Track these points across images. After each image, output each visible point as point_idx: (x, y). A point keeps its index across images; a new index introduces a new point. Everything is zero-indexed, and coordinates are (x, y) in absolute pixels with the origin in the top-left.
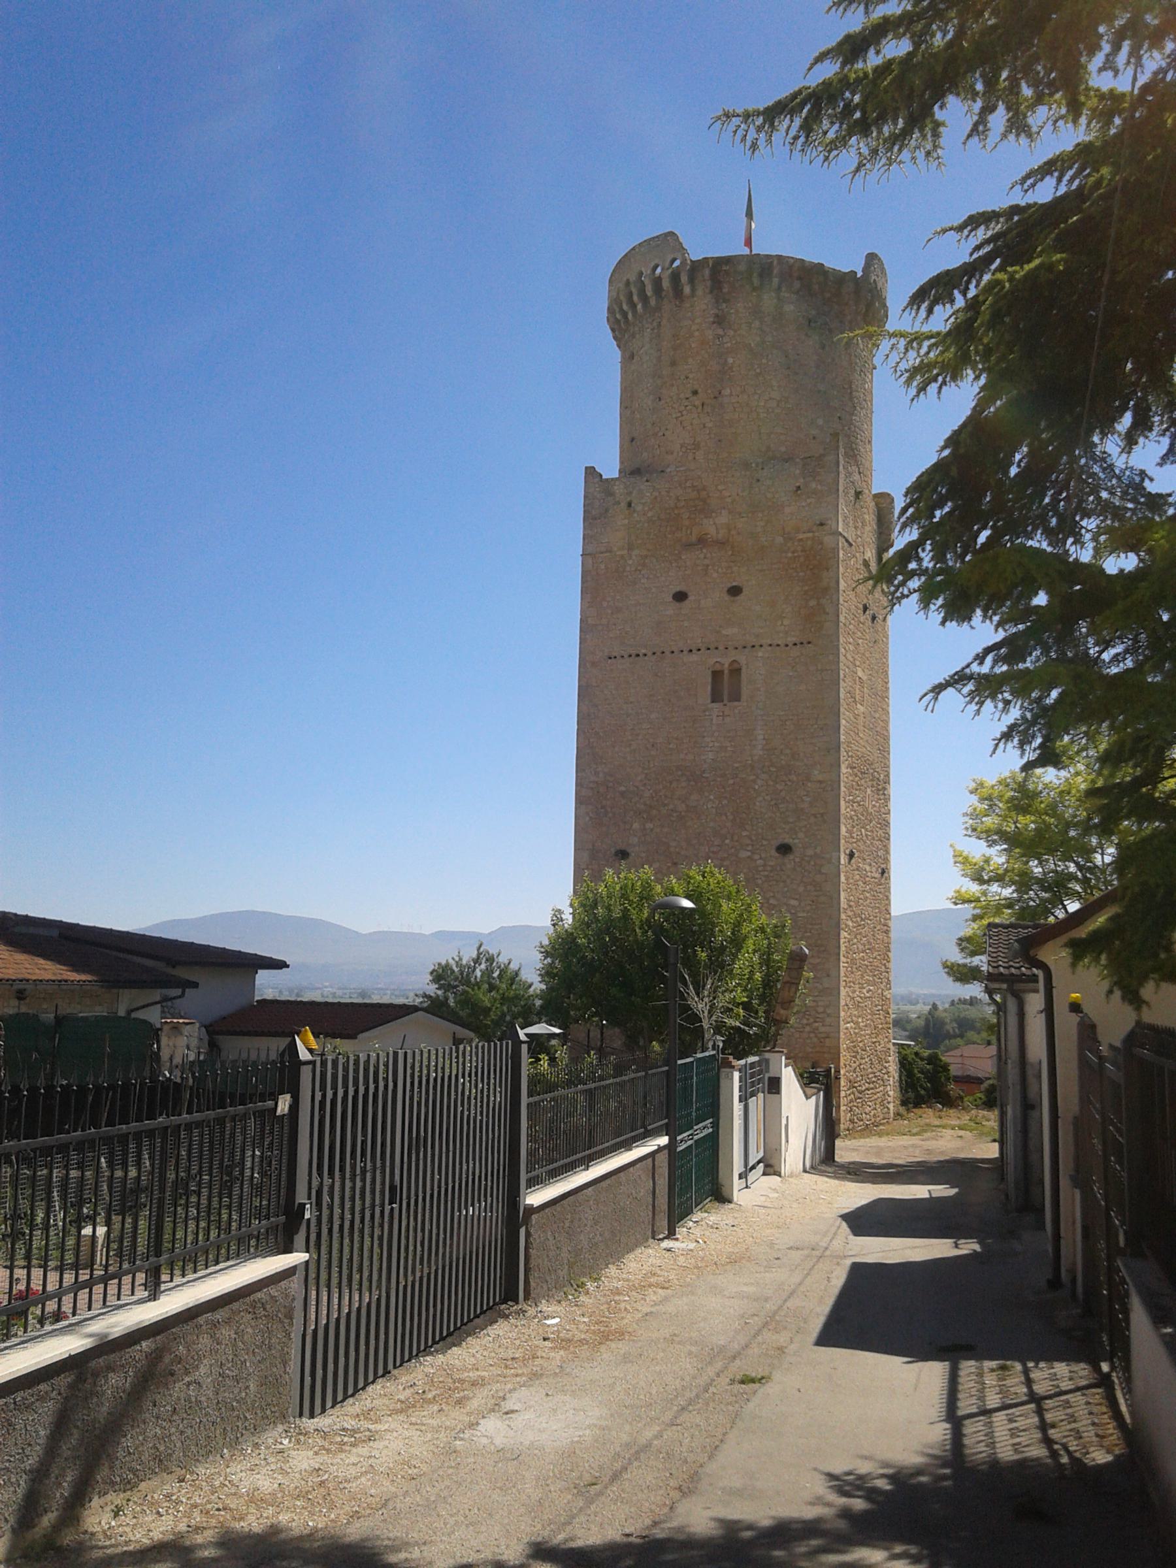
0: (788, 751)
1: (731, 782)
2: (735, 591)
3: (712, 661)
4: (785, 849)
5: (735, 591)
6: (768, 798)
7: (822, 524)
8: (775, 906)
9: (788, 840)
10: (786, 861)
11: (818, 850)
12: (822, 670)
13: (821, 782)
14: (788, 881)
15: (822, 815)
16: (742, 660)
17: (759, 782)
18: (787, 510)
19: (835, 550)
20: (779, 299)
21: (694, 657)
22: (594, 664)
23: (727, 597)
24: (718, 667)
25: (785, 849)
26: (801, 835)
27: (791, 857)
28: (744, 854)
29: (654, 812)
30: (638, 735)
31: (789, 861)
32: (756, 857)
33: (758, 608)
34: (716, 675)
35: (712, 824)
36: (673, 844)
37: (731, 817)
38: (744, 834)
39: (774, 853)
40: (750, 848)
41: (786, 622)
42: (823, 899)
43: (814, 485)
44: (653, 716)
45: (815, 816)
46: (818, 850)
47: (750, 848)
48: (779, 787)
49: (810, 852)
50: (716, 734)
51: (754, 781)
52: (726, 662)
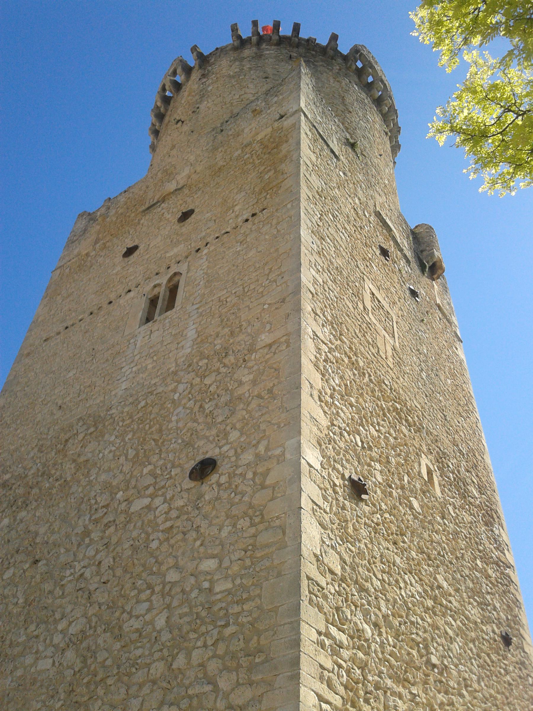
0: (227, 330)
1: (143, 404)
2: (186, 216)
3: (147, 288)
4: (204, 469)
5: (186, 216)
6: (191, 404)
7: (282, 117)
8: (173, 584)
9: (212, 452)
10: (205, 488)
11: (261, 448)
12: (278, 223)
13: (270, 346)
14: (204, 524)
15: (270, 391)
16: (183, 268)
17: (181, 387)
18: (246, 131)
19: (296, 127)
20: (259, 49)
21: (132, 294)
22: (28, 354)
23: (177, 226)
24: (156, 290)
25: (204, 469)
26: (234, 435)
27: (214, 478)
28: (138, 505)
29: (35, 491)
30: (46, 404)
31: (209, 488)
32: (158, 501)
33: (209, 214)
34: (153, 302)
35: (103, 477)
36: (42, 530)
37: (131, 453)
38: (145, 471)
39: (188, 484)
40: (151, 490)
41: (237, 208)
42: (265, 538)
43: (276, 99)
44: (71, 374)
45: (259, 396)
46: (261, 448)
47: (151, 490)
48: (207, 381)
49: (248, 457)
50: (137, 358)
51: (174, 391)
52: (163, 280)
